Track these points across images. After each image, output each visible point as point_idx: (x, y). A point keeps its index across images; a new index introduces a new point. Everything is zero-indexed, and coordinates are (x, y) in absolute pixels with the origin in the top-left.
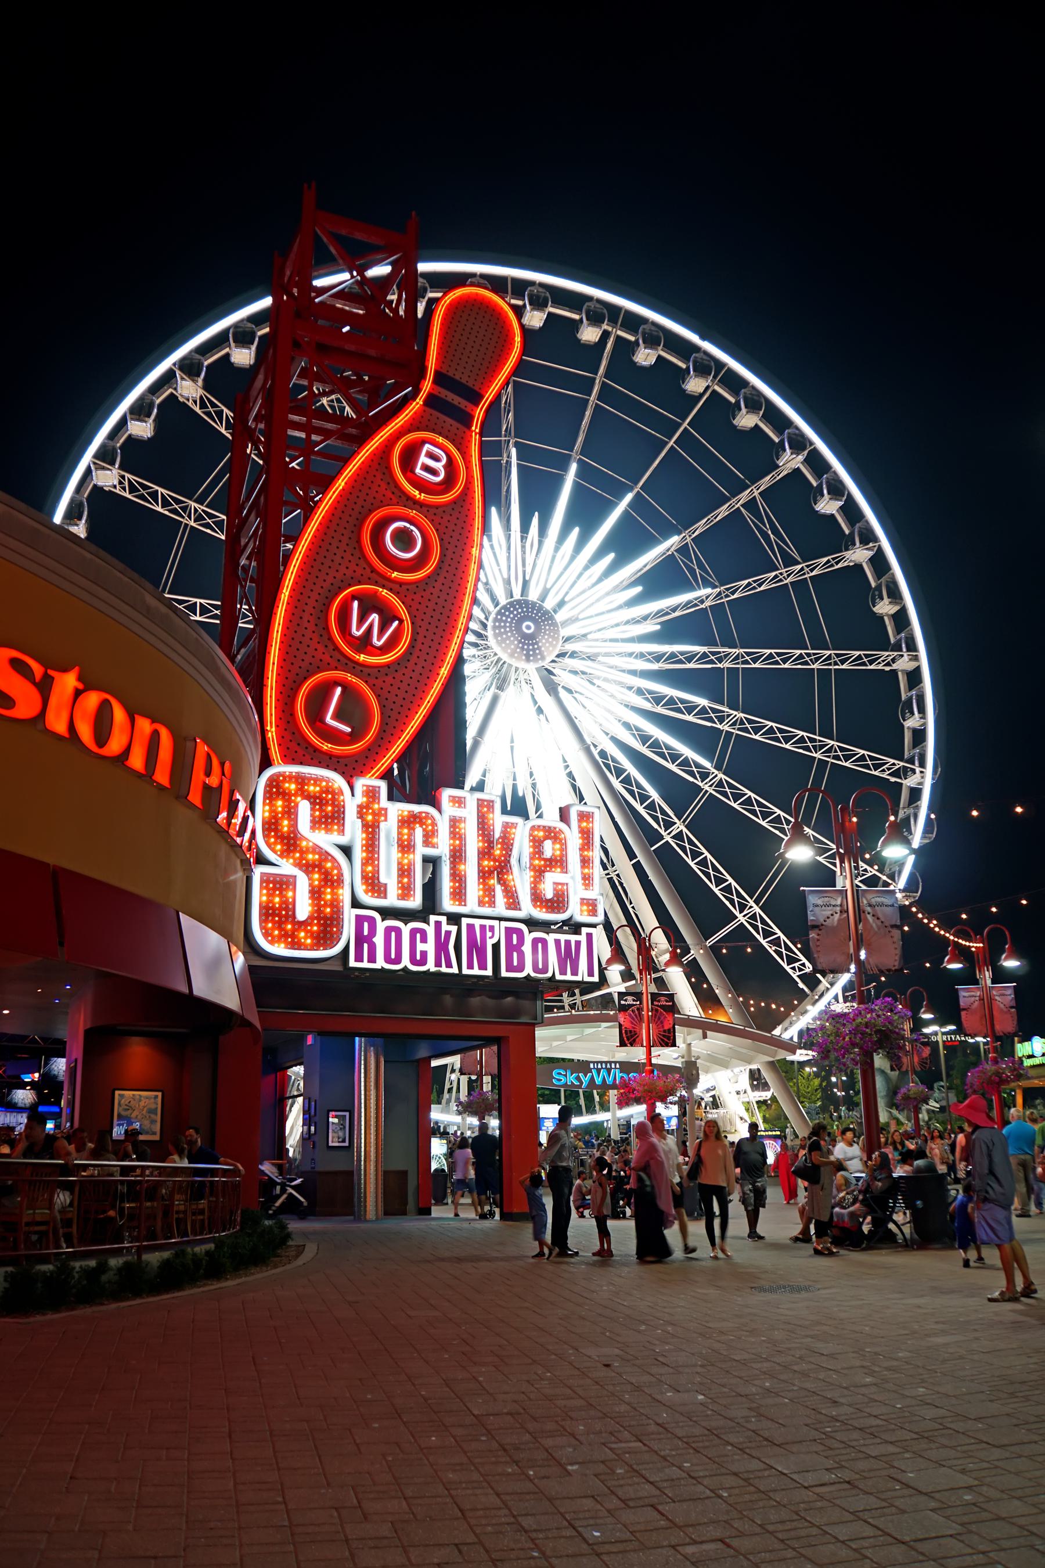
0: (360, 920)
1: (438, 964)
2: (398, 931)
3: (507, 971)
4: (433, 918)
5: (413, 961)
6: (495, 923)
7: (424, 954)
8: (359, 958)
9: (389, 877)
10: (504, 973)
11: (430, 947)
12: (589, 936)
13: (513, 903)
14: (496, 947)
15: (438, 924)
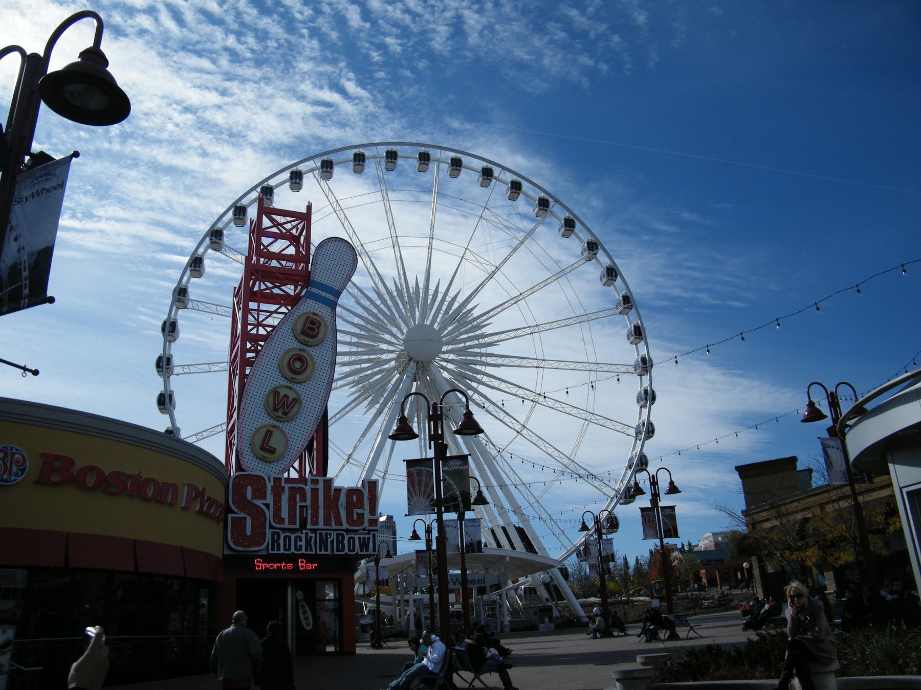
0: (273, 534)
1: (306, 550)
2: (290, 538)
3: (337, 551)
4: (304, 531)
5: (296, 549)
6: (332, 532)
7: (301, 546)
8: (273, 549)
9: (285, 513)
10: (335, 553)
11: (303, 543)
12: (374, 536)
13: (339, 523)
14: (332, 542)
15: (307, 534)
